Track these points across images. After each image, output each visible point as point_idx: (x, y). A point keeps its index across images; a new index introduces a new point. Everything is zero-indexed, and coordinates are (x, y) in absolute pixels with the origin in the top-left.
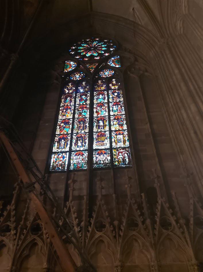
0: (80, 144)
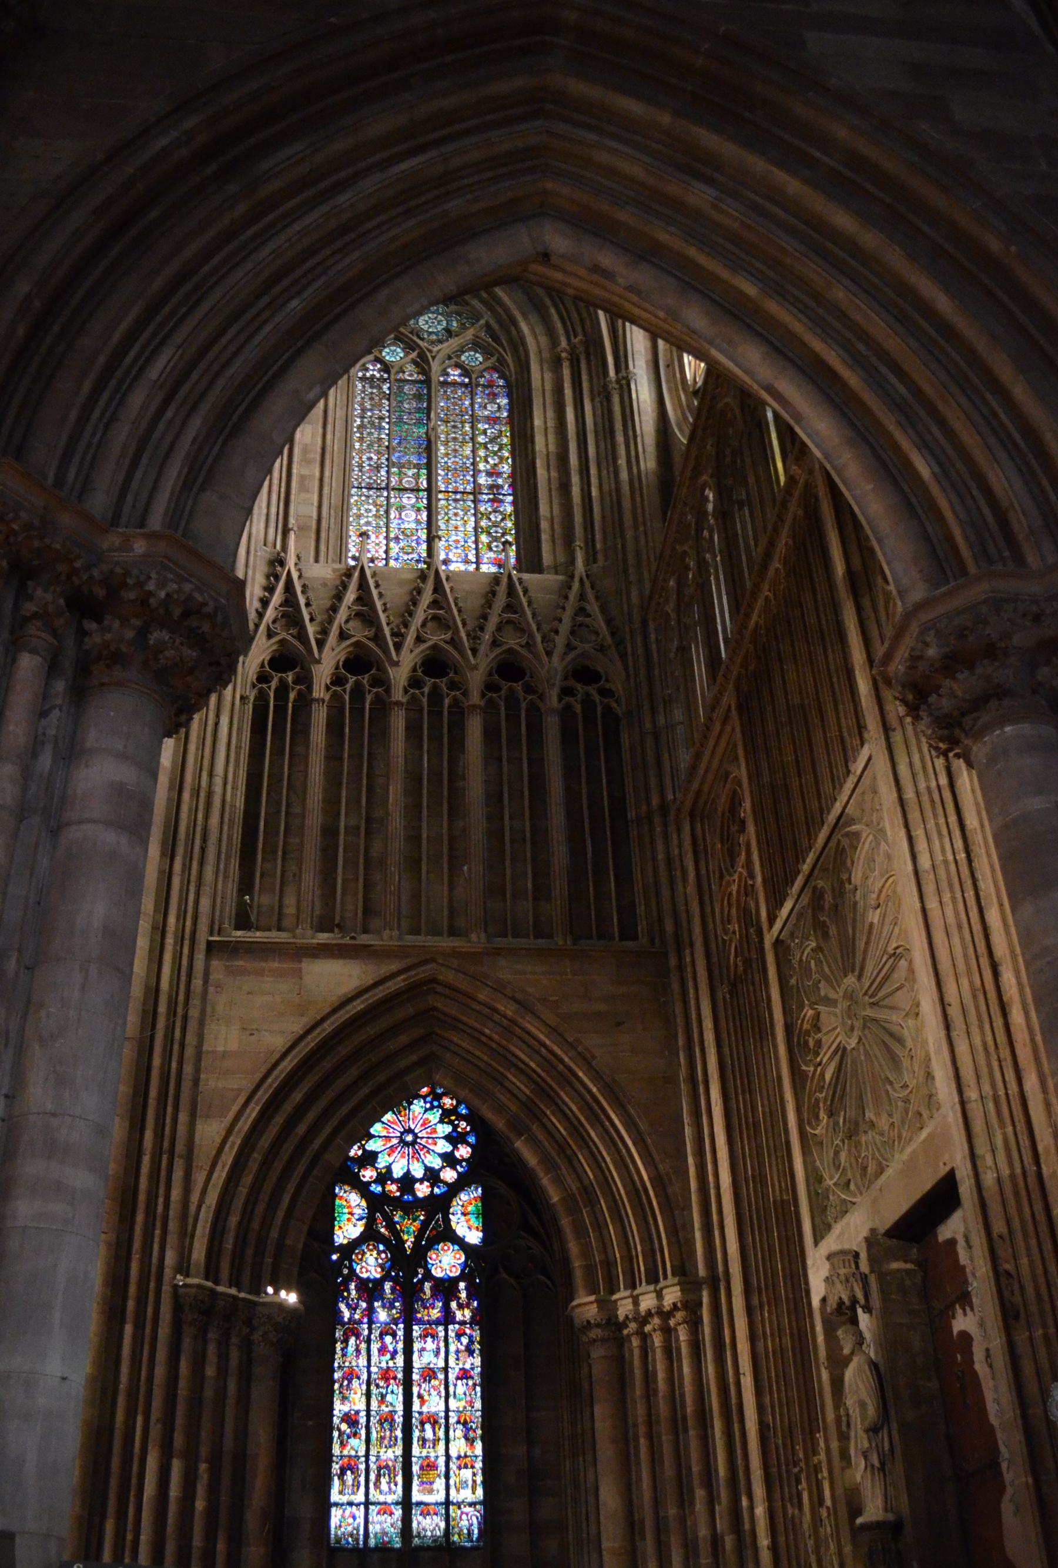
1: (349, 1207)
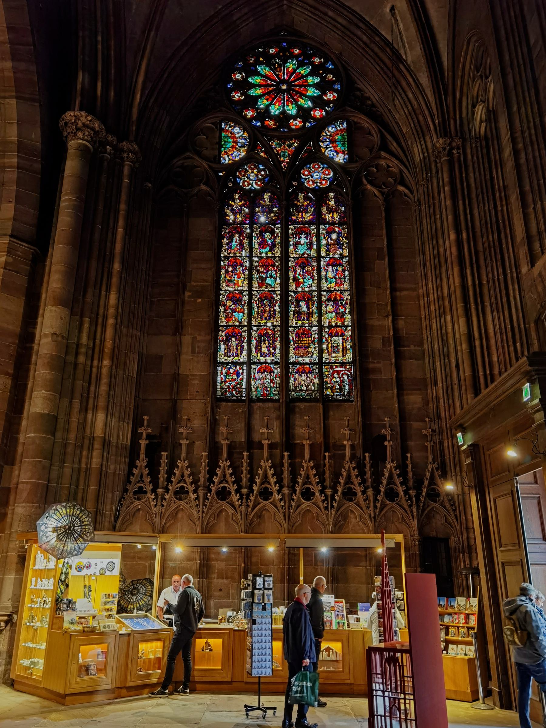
0: (264, 350)
1: (234, 137)
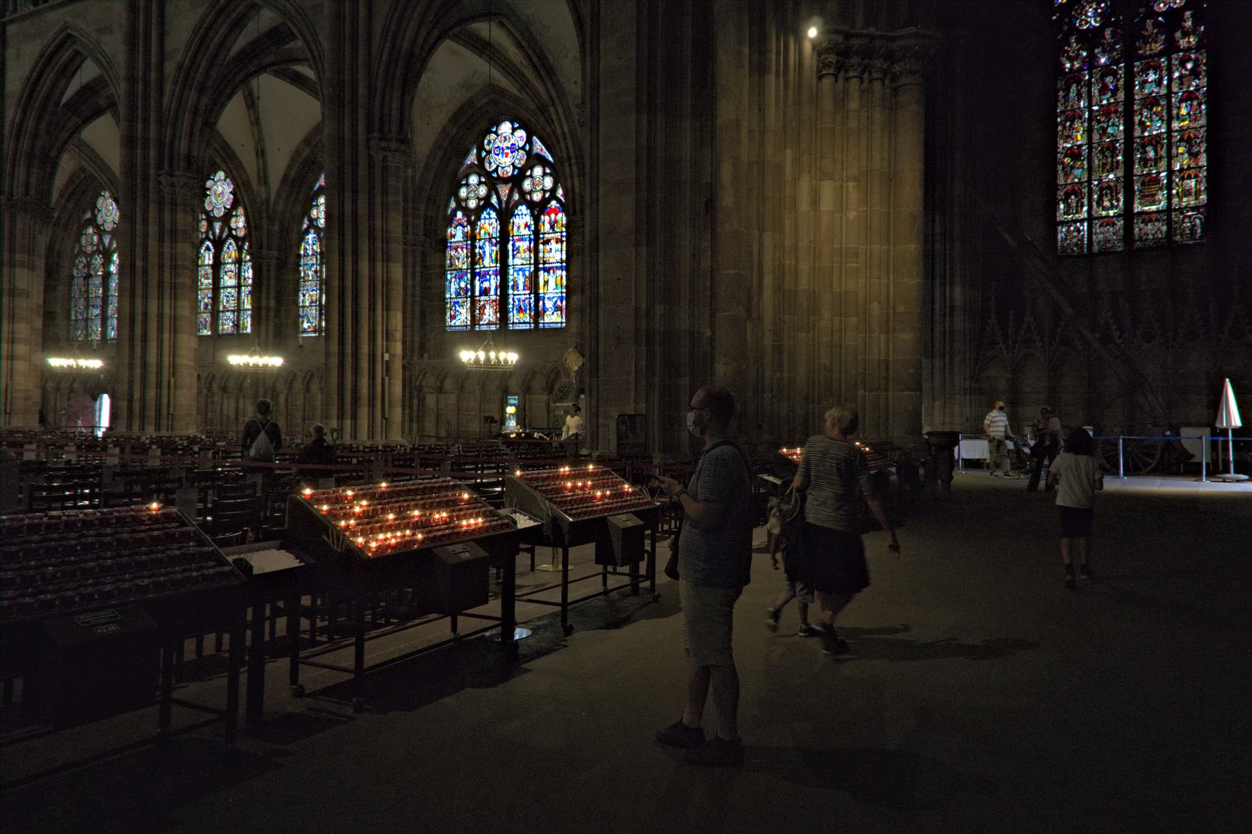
0: (1107, 203)
